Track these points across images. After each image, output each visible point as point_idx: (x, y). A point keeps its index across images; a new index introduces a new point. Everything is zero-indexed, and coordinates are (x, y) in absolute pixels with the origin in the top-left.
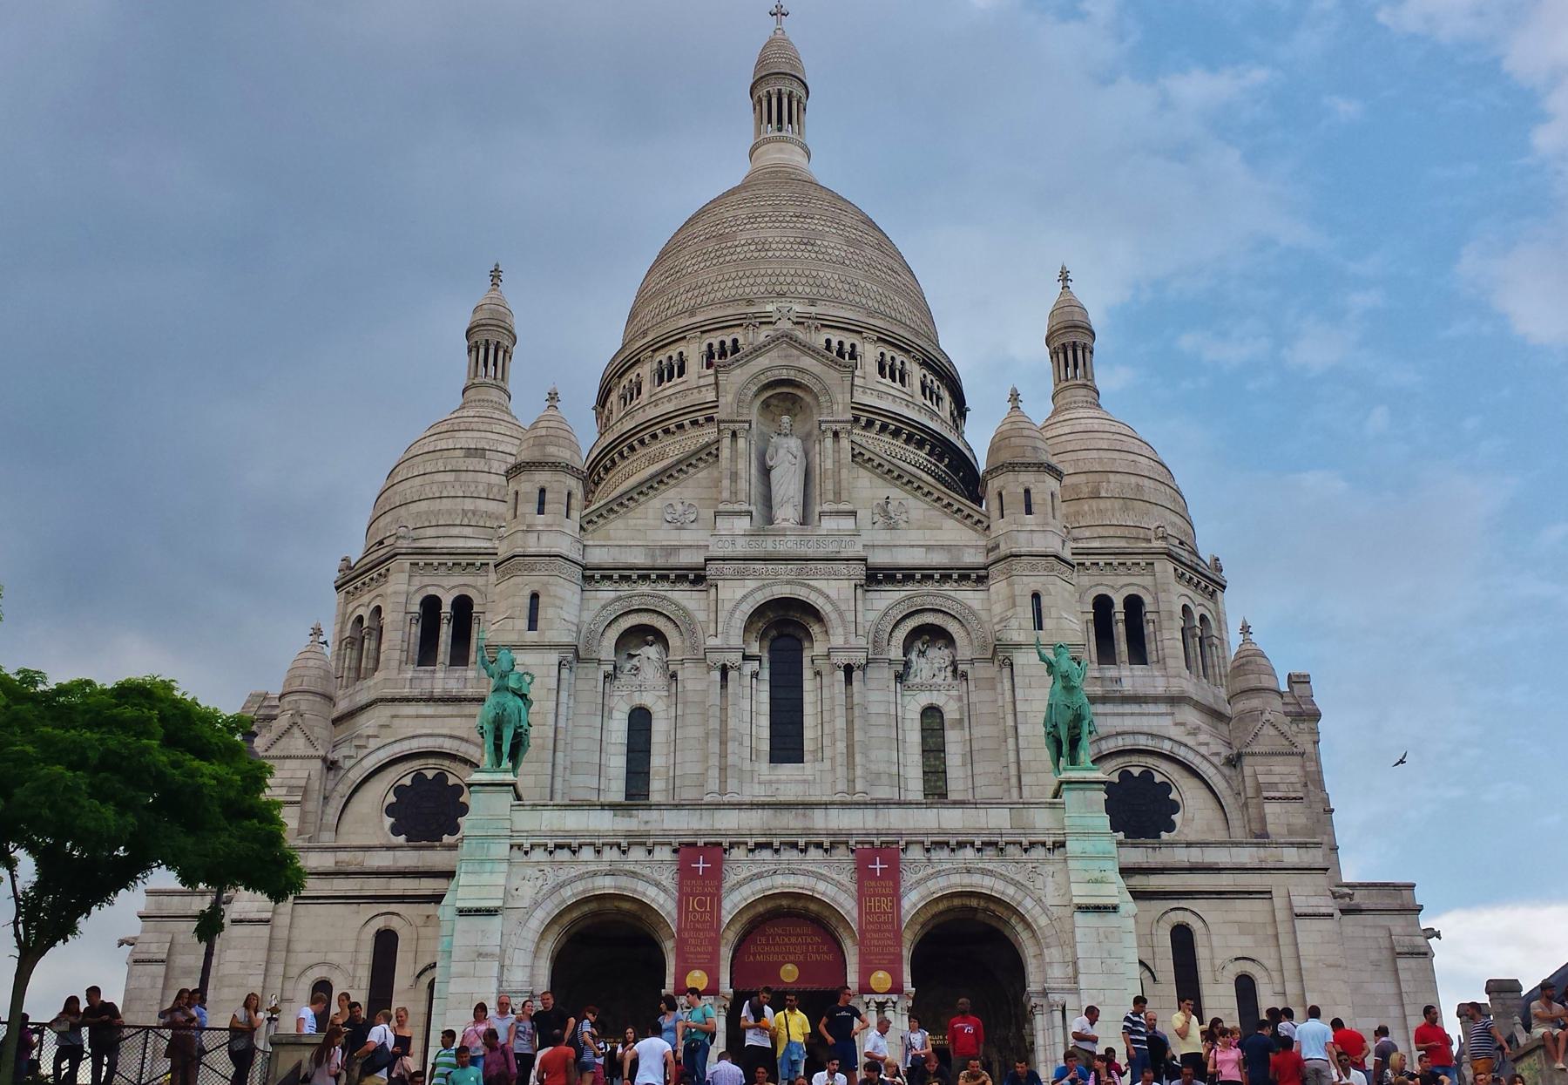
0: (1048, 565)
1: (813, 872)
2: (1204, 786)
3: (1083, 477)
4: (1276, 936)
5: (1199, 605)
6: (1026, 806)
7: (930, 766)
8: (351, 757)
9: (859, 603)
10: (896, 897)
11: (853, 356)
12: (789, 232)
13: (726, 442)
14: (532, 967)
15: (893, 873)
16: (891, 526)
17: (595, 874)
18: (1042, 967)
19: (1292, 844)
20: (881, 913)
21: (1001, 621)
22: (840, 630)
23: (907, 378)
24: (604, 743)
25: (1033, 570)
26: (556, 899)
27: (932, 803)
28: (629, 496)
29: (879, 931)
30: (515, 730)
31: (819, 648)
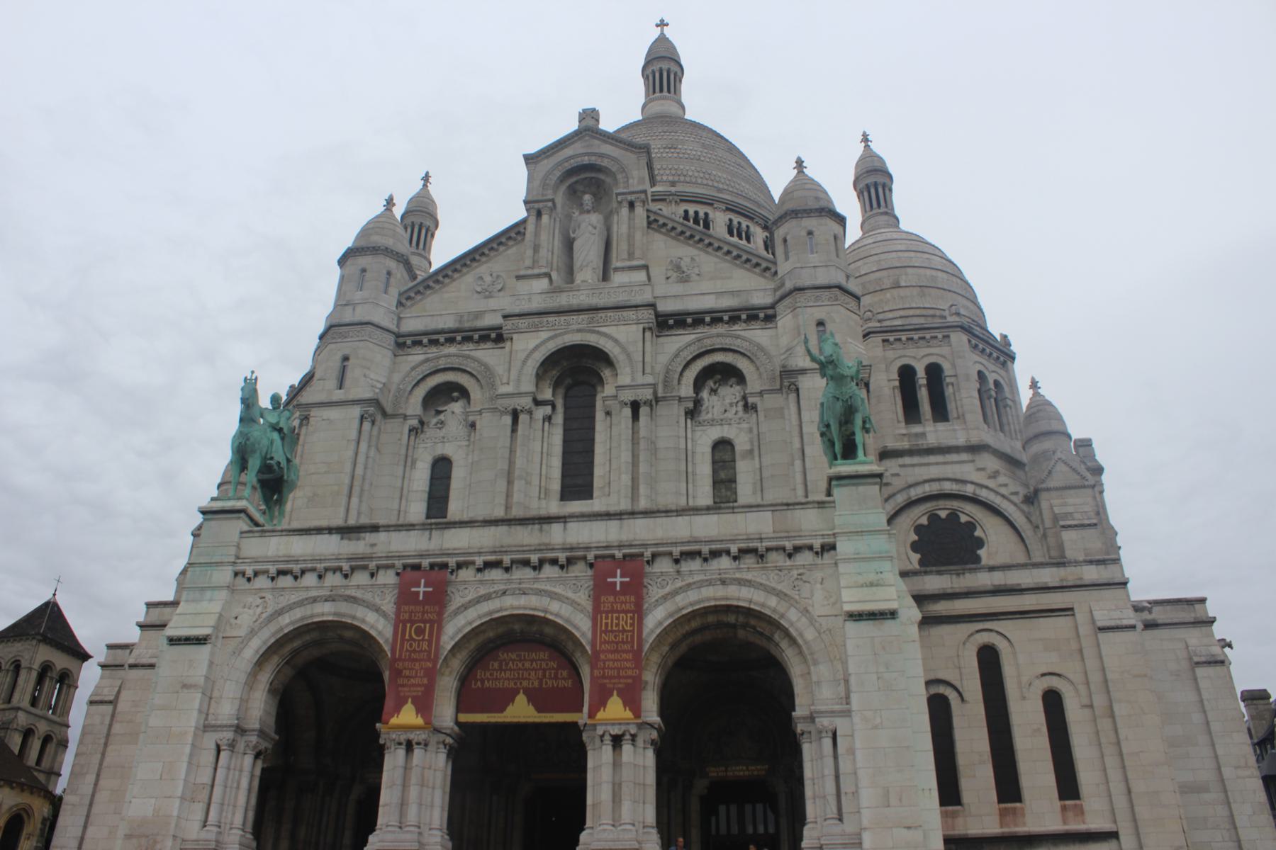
1: (545, 591)
2: (1005, 523)
3: (884, 273)
4: (1081, 651)
5: (993, 372)
9: (648, 344)
10: (639, 612)
15: (636, 588)
16: (684, 279)
17: (314, 600)
19: (1091, 562)
20: (619, 631)
21: (787, 351)
22: (628, 370)
26: (273, 627)
29: (616, 651)
31: (609, 390)
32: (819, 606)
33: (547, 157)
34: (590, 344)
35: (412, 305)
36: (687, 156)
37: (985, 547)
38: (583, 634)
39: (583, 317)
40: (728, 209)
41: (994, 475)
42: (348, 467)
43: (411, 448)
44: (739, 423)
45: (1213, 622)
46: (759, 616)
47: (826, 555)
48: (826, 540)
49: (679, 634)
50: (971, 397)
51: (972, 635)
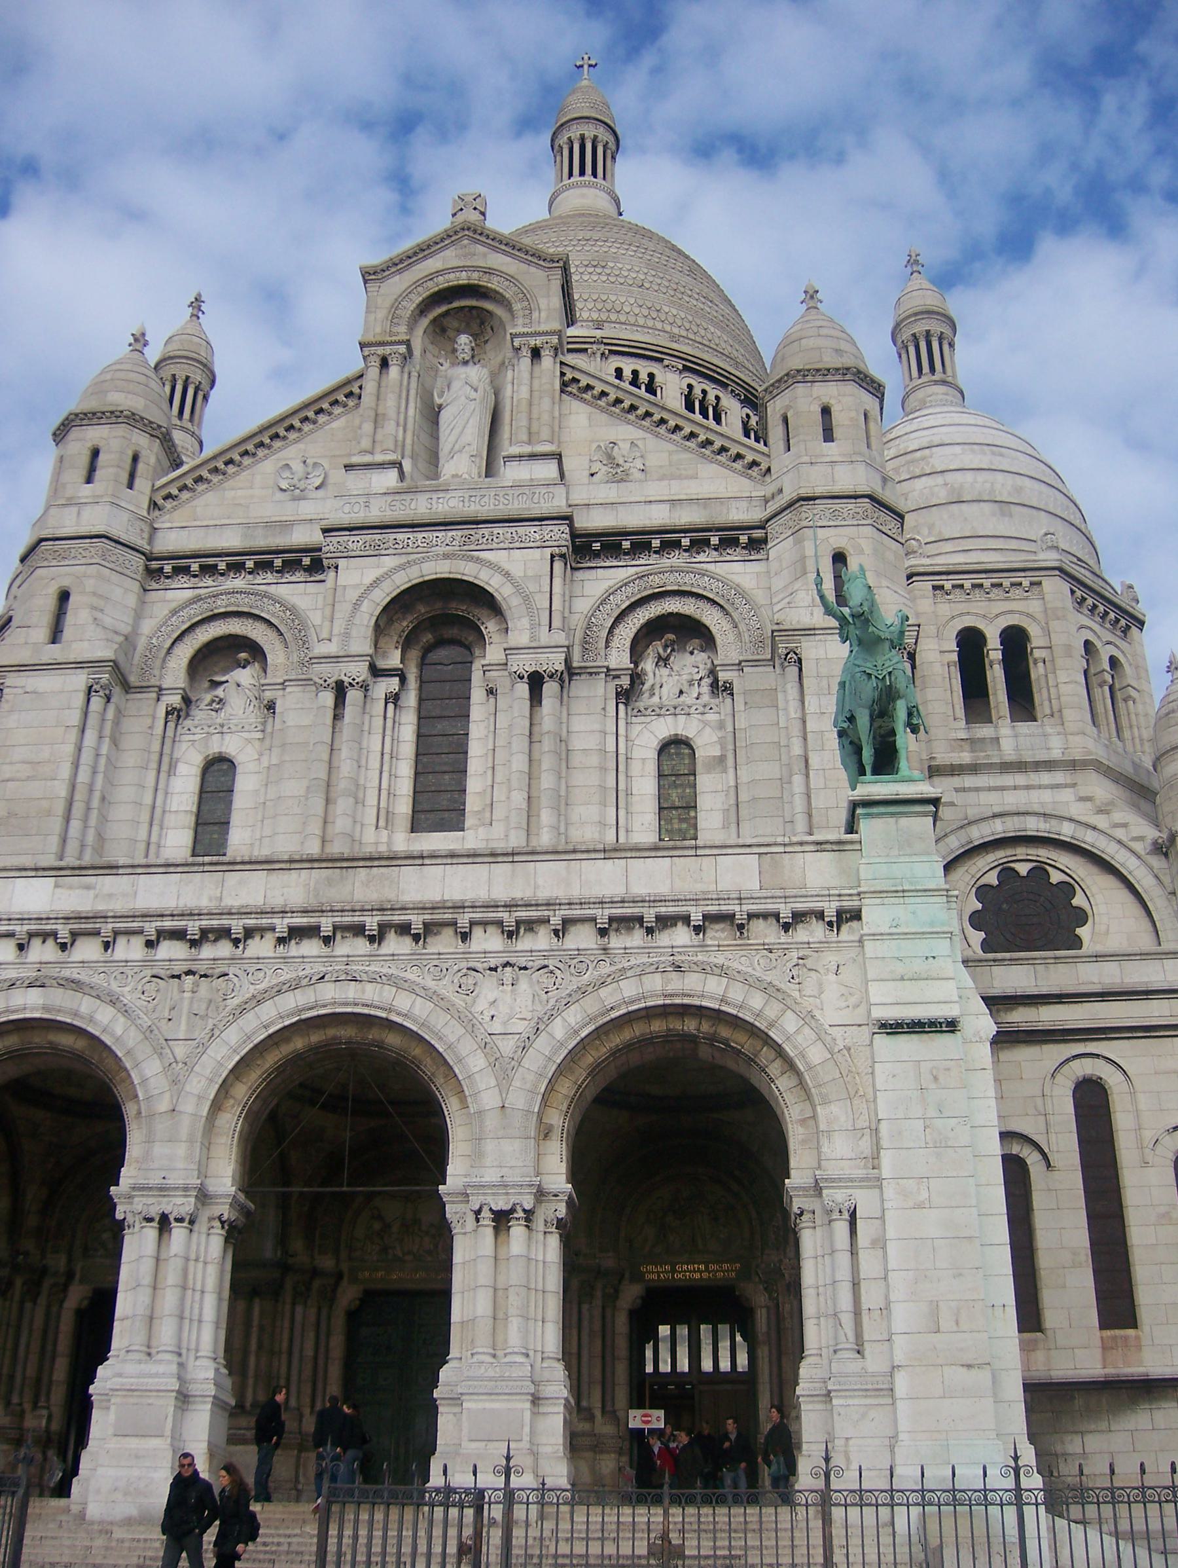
0: (858, 510)
1: (390, 977)
6: (788, 849)
9: (557, 581)
11: (651, 389)
16: (619, 476)
18: (816, 1138)
22: (525, 622)
23: (723, 416)
25: (836, 517)
31: (493, 653)
33: (400, 271)
34: (465, 578)
35: (174, 508)
36: (622, 281)
39: (457, 533)
40: (686, 369)
42: (65, 771)
43: (168, 742)
46: (736, 1022)
47: (845, 928)
48: (844, 904)
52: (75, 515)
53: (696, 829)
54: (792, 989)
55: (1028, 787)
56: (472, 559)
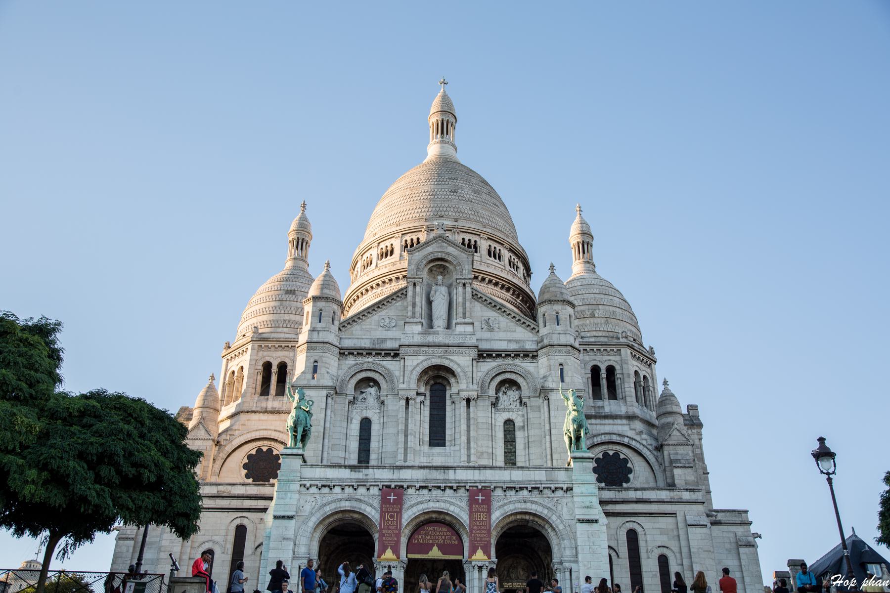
1: (448, 501)
4: (679, 536)
7: (507, 449)
8: (226, 440)
9: (474, 368)
10: (489, 512)
11: (475, 247)
12: (445, 187)
13: (410, 288)
14: (309, 545)
15: (488, 502)
16: (491, 329)
19: (687, 490)
23: (502, 257)
24: (348, 436)
25: (560, 352)
26: (322, 512)
27: (507, 468)
28: (363, 314)
29: (480, 530)
30: (304, 428)
31: (454, 390)
32: (565, 515)
33: (419, 251)
37: (633, 473)
38: (465, 521)
41: (641, 433)
43: (350, 413)
44: (517, 411)
45: (751, 524)
47: (568, 492)
49: (505, 523)
50: (630, 387)
51: (624, 523)
52: (317, 335)
53: (515, 448)
54: (555, 508)
55: (613, 424)
56: (447, 359)
